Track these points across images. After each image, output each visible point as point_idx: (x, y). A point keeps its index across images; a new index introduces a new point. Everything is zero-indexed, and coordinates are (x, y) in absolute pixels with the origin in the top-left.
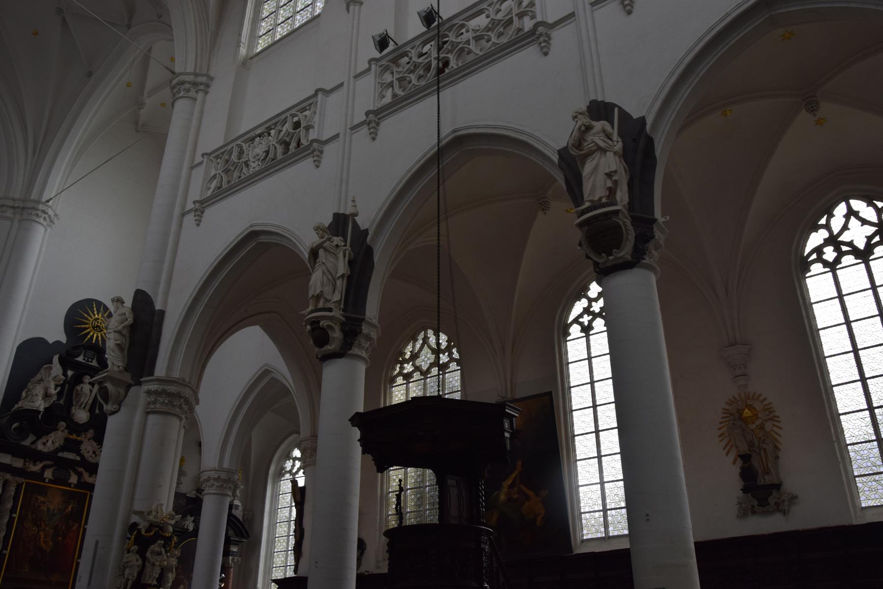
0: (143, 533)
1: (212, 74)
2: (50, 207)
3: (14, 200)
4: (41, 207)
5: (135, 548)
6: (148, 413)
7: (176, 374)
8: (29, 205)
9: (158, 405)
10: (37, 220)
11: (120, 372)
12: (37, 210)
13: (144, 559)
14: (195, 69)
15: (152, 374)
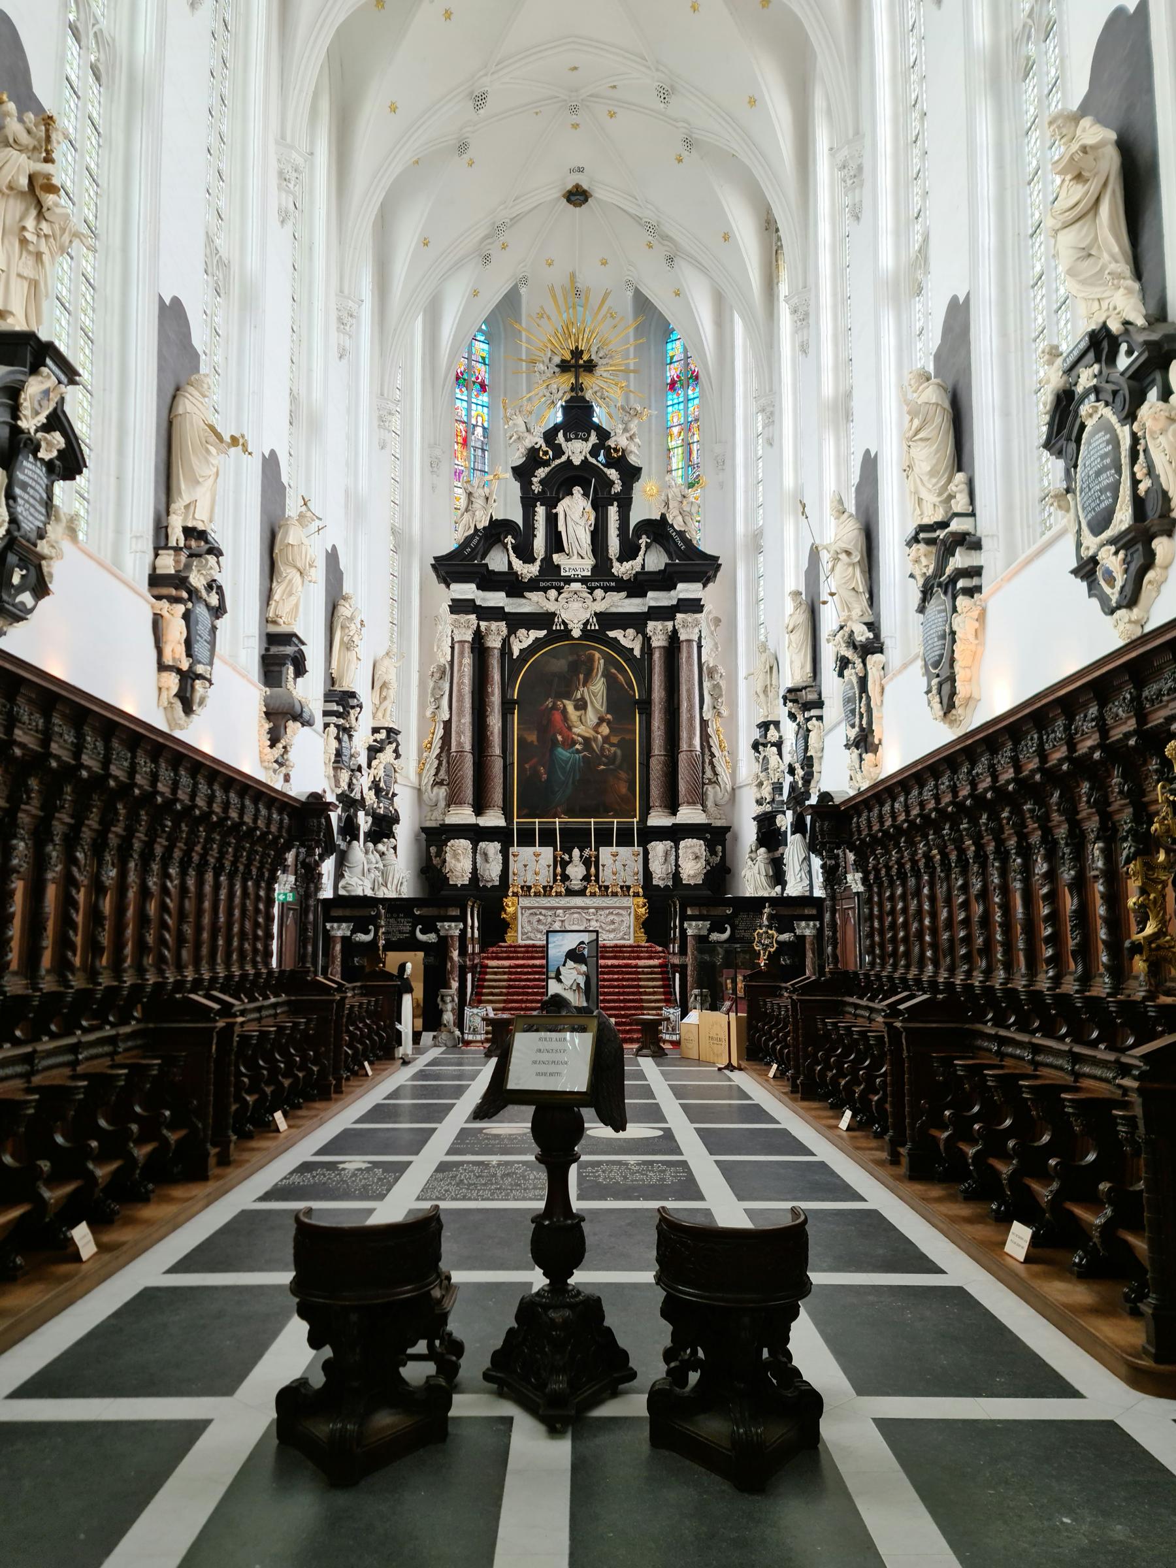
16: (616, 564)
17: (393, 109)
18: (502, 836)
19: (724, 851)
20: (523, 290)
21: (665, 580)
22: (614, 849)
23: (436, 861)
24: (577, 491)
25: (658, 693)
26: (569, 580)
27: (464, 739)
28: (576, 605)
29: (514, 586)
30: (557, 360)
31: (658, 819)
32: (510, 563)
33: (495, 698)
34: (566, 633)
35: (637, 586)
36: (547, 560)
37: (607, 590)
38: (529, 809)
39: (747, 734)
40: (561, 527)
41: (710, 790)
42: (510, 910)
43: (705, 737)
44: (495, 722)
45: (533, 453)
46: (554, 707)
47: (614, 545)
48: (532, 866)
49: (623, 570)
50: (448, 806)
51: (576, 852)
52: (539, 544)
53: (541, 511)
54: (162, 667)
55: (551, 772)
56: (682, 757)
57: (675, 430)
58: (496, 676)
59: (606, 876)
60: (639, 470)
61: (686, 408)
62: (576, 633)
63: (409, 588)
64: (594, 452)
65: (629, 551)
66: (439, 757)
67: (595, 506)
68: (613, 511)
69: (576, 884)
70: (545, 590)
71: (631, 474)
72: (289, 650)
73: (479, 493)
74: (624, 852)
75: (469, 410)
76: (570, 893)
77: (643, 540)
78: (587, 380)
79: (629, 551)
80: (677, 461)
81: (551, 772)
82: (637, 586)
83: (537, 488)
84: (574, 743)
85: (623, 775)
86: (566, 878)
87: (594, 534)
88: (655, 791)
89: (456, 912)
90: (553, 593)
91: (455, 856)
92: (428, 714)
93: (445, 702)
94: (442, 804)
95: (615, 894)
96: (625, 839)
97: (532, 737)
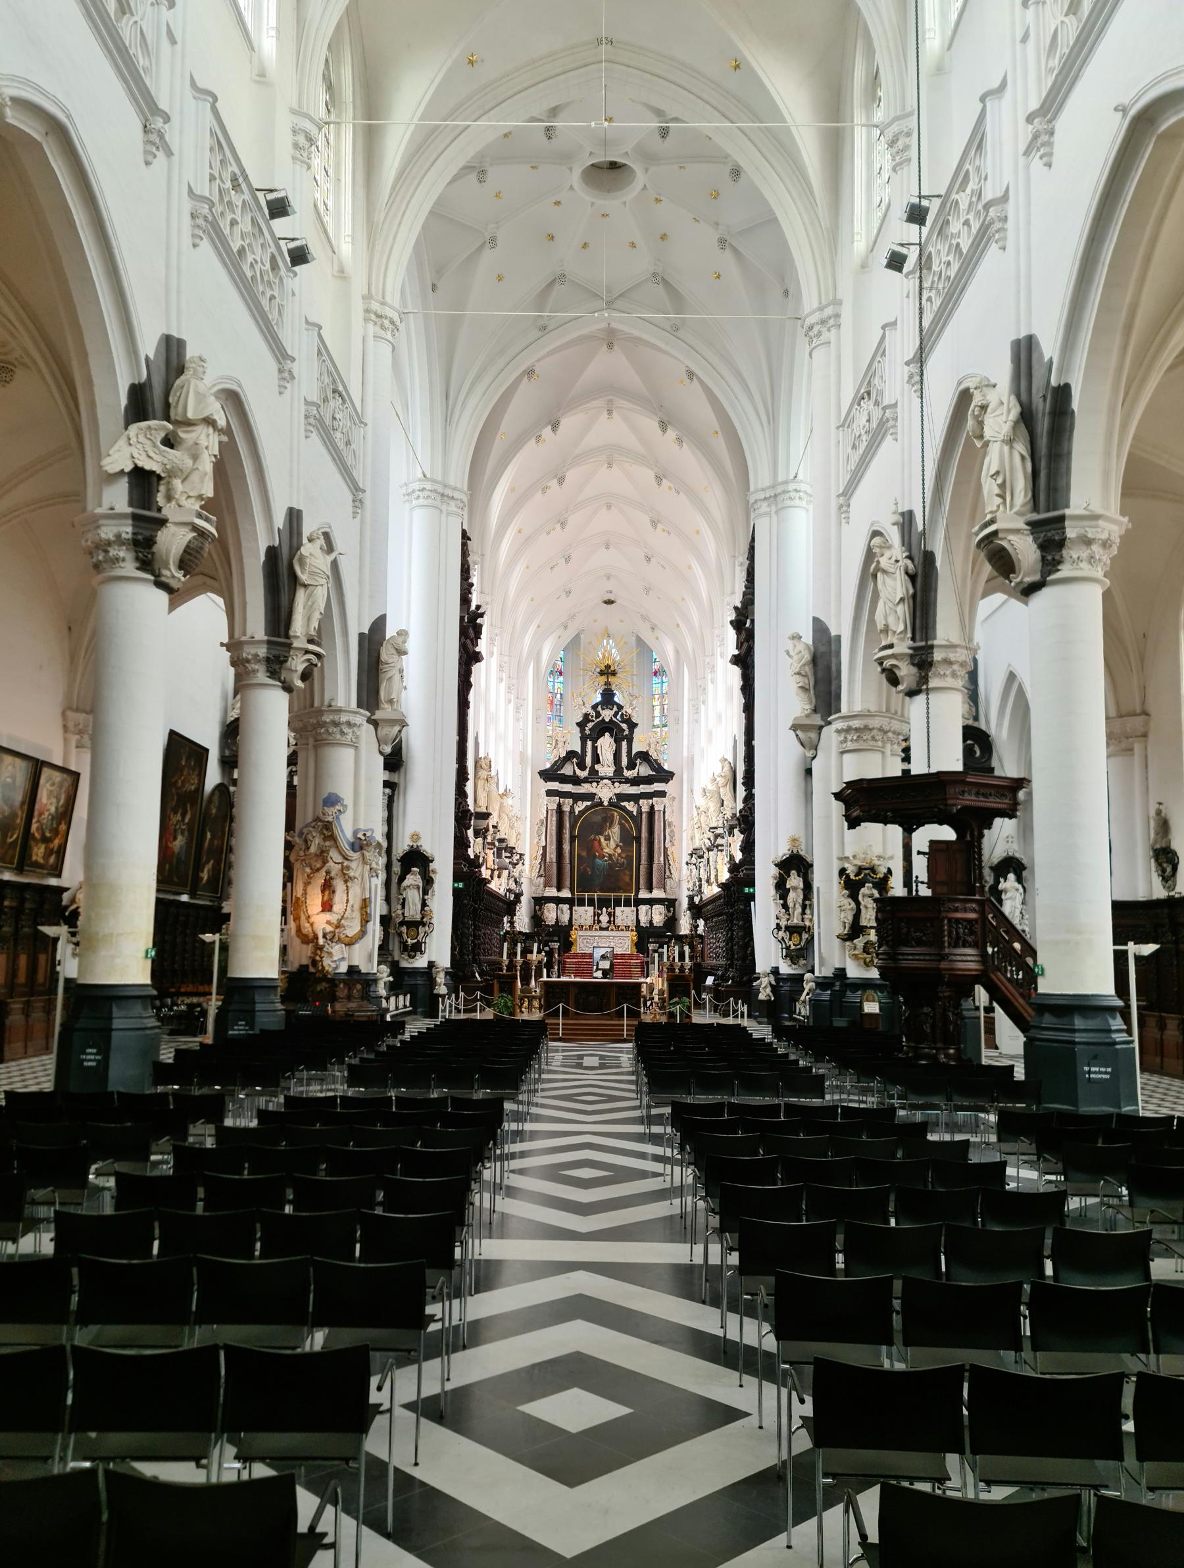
0: (852, 877)
1: (839, 296)
2: (801, 481)
3: (763, 490)
4: (791, 487)
5: (846, 892)
6: (842, 753)
7: (858, 708)
8: (779, 490)
9: (849, 743)
10: (792, 503)
11: (807, 716)
12: (788, 492)
13: (858, 904)
14: (820, 303)
15: (839, 710)
16: (625, 771)
17: (532, 600)
18: (570, 902)
19: (674, 910)
20: (582, 636)
21: (648, 780)
22: (622, 908)
23: (539, 913)
24: (607, 734)
25: (644, 834)
26: (602, 778)
27: (552, 856)
28: (606, 790)
29: (576, 781)
30: (598, 670)
31: (643, 895)
32: (574, 771)
33: (567, 836)
34: (601, 804)
35: (636, 782)
36: (592, 768)
37: (620, 783)
38: (582, 888)
39: (686, 858)
40: (599, 752)
41: (668, 881)
42: (574, 937)
43: (666, 856)
44: (566, 847)
45: (586, 716)
46: (595, 839)
47: (625, 761)
48: (584, 916)
49: (628, 774)
50: (545, 887)
51: (604, 909)
52: (589, 760)
53: (589, 743)
54: (487, 868)
55: (593, 870)
56: (655, 866)
57: (657, 697)
58: (567, 825)
59: (618, 922)
60: (637, 725)
61: (662, 687)
62: (606, 803)
63: (526, 781)
64: (615, 715)
65: (631, 766)
66: (540, 863)
67: (615, 741)
68: (624, 744)
69: (604, 925)
70: (591, 782)
71: (633, 726)
72: (504, 845)
73: (561, 740)
74: (627, 909)
75: (554, 686)
76: (602, 929)
77: (638, 761)
78: (611, 679)
79: (631, 766)
80: (657, 712)
81: (593, 870)
82: (636, 782)
83: (588, 732)
84: (604, 856)
85: (627, 872)
86: (599, 922)
87: (615, 755)
88: (642, 881)
89: (556, 938)
90: (595, 784)
91: (549, 911)
92: (536, 841)
93: (543, 837)
94: (542, 886)
95: (622, 930)
96: (627, 903)
97: (584, 854)
